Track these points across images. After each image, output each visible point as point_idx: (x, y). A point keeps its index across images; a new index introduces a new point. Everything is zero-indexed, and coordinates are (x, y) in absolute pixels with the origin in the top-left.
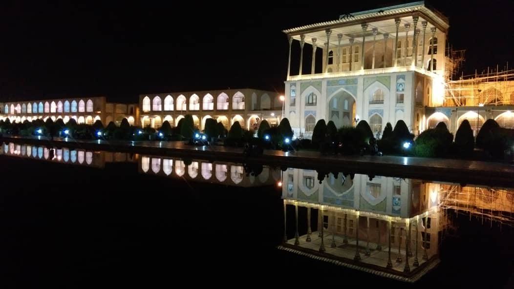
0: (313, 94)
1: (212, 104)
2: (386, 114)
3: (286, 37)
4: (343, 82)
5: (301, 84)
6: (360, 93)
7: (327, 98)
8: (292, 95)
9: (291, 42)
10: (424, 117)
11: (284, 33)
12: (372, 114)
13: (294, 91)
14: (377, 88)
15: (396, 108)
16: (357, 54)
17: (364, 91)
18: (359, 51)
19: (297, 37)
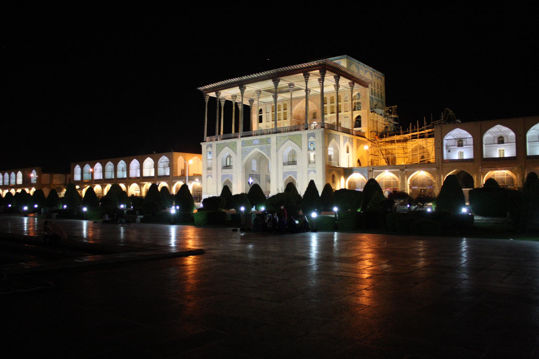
0: (230, 157)
1: (153, 170)
2: (298, 175)
3: (202, 95)
4: (257, 142)
5: (217, 144)
6: (273, 154)
7: (242, 160)
8: (209, 158)
9: (207, 100)
10: (342, 178)
11: (200, 91)
12: (286, 176)
13: (210, 153)
14: (290, 149)
15: (309, 169)
16: (285, 111)
17: (277, 151)
18: (287, 108)
19: (213, 94)
